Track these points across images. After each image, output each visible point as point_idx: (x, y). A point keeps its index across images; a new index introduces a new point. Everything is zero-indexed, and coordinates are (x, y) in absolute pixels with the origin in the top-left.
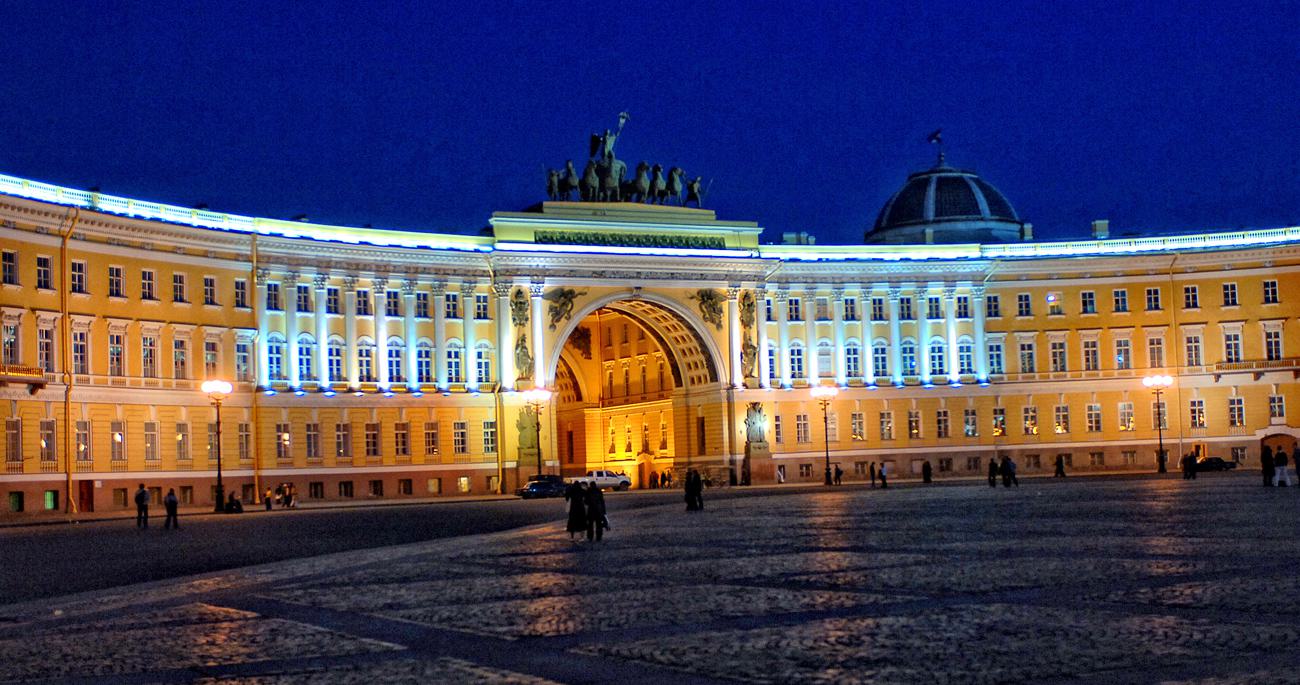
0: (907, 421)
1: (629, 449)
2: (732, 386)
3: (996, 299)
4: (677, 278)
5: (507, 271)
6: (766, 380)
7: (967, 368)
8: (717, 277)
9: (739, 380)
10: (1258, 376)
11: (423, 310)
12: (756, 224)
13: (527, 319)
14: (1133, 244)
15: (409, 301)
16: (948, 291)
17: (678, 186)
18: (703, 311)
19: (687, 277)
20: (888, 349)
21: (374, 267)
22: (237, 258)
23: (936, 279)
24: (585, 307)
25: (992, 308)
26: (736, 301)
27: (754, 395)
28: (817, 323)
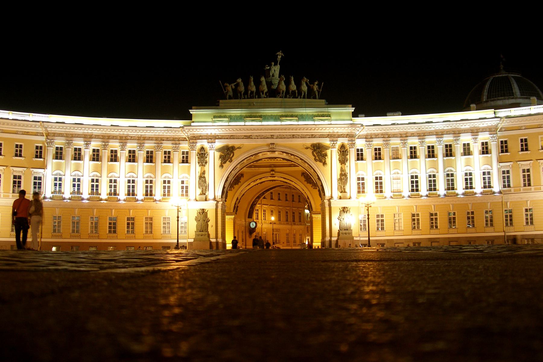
3: (506, 142)
4: (296, 138)
5: (194, 137)
7: (487, 185)
8: (322, 136)
11: (150, 158)
12: (351, 105)
13: (206, 163)
15: (141, 155)
17: (304, 88)
18: (314, 156)
19: (303, 137)
20: (437, 174)
21: (118, 137)
22: (36, 134)
23: (465, 131)
24: (241, 155)
25: (504, 147)
27: (344, 203)
28: (392, 161)
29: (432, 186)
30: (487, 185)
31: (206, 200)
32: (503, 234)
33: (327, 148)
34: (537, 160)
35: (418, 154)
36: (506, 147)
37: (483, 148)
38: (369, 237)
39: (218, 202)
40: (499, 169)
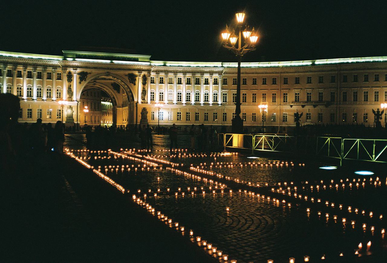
0: (195, 116)
1: (126, 120)
2: (138, 102)
5: (65, 66)
6: (149, 101)
7: (215, 100)
8: (135, 70)
10: (303, 106)
13: (72, 80)
14: (269, 64)
16: (210, 76)
18: (129, 79)
23: (207, 72)
25: (225, 82)
26: (141, 77)
28: (168, 85)
29: (188, 99)
30: (215, 100)
31: (72, 101)
33: (136, 76)
35: (182, 82)
36: (226, 82)
37: (215, 82)
38: (159, 123)
40: (221, 93)
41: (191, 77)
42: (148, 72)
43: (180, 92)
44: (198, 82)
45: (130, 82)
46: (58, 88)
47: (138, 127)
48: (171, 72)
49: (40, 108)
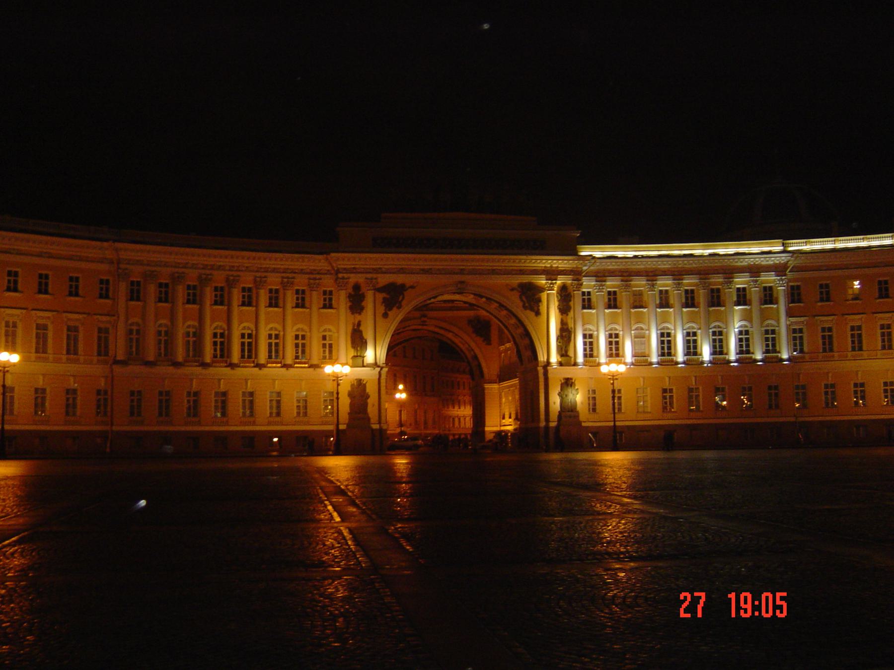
1: (510, 418)
2: (548, 363)
4: (498, 274)
6: (580, 359)
8: (536, 272)
9: (554, 358)
16: (753, 281)
18: (522, 300)
25: (794, 295)
27: (568, 372)
29: (692, 348)
31: (363, 366)
32: (792, 419)
33: (541, 289)
34: (843, 315)
35: (672, 302)
37: (765, 295)
38: (615, 421)
39: (382, 368)
40: (788, 326)
41: (696, 285)
42: (576, 277)
43: (665, 331)
44: (716, 299)
45: (525, 307)
46: (325, 330)
47: (551, 435)
48: (638, 273)
49: (277, 389)
